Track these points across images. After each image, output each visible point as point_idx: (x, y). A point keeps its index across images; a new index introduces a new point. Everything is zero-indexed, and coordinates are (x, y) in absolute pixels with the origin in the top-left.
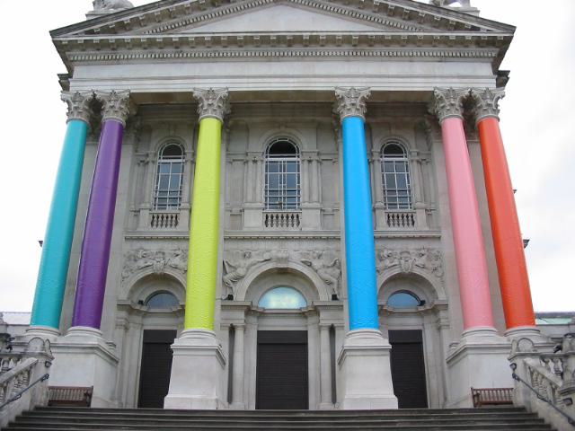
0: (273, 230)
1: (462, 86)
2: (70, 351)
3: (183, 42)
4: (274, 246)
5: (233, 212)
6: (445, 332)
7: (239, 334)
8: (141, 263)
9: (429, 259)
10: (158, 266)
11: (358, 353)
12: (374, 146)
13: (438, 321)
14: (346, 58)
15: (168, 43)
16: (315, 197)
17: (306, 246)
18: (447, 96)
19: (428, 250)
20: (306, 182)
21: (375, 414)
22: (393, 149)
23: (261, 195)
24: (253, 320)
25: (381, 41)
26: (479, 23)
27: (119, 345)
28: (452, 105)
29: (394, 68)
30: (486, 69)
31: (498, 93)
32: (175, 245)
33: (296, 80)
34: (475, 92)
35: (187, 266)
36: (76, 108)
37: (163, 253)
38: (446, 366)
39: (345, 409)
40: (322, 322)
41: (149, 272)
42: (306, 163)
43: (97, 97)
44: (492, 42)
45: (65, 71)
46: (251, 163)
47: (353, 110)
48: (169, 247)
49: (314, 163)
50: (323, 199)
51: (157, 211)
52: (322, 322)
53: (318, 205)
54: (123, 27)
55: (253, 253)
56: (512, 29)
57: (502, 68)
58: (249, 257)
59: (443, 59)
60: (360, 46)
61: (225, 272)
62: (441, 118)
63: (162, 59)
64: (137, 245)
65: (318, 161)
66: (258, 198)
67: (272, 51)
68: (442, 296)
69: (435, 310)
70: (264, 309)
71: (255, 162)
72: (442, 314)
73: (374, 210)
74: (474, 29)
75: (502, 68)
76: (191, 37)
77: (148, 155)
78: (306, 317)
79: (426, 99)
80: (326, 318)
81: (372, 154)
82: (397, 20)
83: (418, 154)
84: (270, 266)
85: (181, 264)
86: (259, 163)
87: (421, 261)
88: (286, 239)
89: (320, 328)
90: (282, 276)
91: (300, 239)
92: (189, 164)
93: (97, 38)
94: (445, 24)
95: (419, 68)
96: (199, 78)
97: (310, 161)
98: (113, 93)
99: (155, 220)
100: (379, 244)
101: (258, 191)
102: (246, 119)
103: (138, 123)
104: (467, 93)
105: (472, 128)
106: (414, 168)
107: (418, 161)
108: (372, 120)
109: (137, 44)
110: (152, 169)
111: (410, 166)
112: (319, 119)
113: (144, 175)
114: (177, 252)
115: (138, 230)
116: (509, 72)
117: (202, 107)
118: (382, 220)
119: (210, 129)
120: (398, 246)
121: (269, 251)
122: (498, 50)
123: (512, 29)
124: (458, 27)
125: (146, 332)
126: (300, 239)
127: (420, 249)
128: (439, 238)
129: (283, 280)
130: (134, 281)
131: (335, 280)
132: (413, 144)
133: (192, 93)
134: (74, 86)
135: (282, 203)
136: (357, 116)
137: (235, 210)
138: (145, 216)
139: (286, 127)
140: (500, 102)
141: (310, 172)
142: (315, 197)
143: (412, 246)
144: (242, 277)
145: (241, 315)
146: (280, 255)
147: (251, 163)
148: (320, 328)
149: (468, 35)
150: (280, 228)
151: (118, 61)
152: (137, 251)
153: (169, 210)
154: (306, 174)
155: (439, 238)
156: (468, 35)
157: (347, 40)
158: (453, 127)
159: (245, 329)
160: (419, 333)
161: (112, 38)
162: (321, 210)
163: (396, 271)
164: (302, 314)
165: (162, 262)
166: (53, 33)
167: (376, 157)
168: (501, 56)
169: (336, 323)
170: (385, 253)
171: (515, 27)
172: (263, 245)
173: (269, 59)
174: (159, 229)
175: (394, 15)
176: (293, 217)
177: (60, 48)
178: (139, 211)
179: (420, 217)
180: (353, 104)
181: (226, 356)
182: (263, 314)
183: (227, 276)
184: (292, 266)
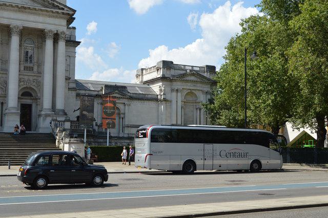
6: (38, 106)
29: (32, 18)
30: (64, 22)
44: (68, 14)
56: (75, 11)
59: (50, 16)
69: (36, 99)
72: (38, 100)
95: (40, 19)
120: (26, 78)
123: (75, 11)
149: (60, 11)
158: (49, 44)
170: (22, 80)
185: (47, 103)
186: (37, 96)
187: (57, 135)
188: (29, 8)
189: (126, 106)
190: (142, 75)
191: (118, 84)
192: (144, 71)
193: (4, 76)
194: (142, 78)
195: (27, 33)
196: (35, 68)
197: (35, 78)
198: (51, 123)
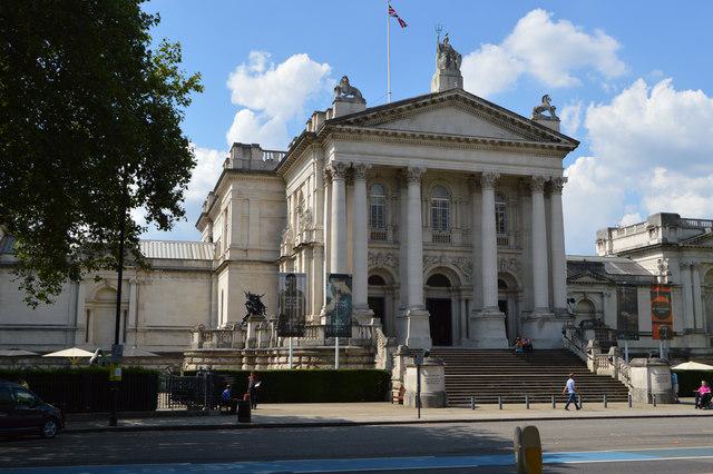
4: (439, 254)
6: (520, 304)
17: (454, 254)
29: (511, 158)
59: (538, 154)
74: (559, 141)
95: (523, 159)
185: (541, 300)
186: (517, 286)
187: (590, 352)
188: (510, 144)
189: (606, 299)
190: (611, 240)
191: (588, 259)
192: (614, 233)
193: (467, 255)
194: (611, 246)
195: (436, 179)
196: (390, 236)
197: (513, 256)
198: (564, 332)
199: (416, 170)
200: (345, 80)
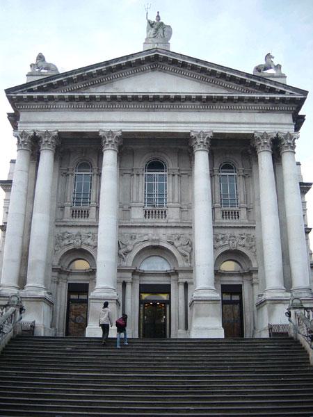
0: (150, 221)
1: (271, 130)
2: (28, 299)
3: (92, 98)
4: (151, 231)
5: (124, 208)
7: (129, 287)
8: (66, 242)
9: (247, 241)
10: (77, 243)
11: (201, 302)
12: (215, 165)
13: (252, 280)
14: (198, 110)
15: (82, 99)
16: (176, 199)
17: (170, 231)
18: (262, 137)
19: (247, 235)
20: (171, 189)
21: (211, 341)
22: (227, 167)
23: (141, 198)
24: (137, 277)
25: (220, 99)
26: (285, 88)
27: (54, 294)
28: (265, 143)
29: (228, 117)
30: (288, 119)
31: (295, 135)
32: (88, 230)
33: (165, 125)
34: (280, 135)
35: (97, 243)
36: (23, 142)
37: (81, 236)
38: (255, 308)
39: (193, 338)
40: (180, 280)
41: (71, 247)
42: (171, 176)
43: (37, 135)
44: (293, 101)
45: (12, 111)
46: (135, 176)
47: (202, 146)
48: (84, 231)
49: (176, 176)
50: (181, 200)
51: (75, 207)
52: (180, 280)
53: (179, 205)
54: (51, 87)
55: (137, 236)
56: (305, 93)
57: (300, 113)
58: (135, 239)
60: (208, 103)
61: (120, 248)
62: (258, 151)
63: (78, 109)
64: (64, 230)
65: (178, 175)
66: (140, 200)
67: (149, 105)
68: (254, 265)
70: (144, 271)
71: (138, 175)
72: (254, 276)
73: (213, 208)
75: (300, 113)
76: (97, 95)
77: (68, 170)
78: (170, 276)
79: (248, 138)
80: (182, 278)
81: (213, 171)
82: (233, 85)
83: (243, 171)
84: (148, 244)
85: (92, 243)
86: (141, 176)
87: (243, 242)
88: (158, 227)
89: (178, 284)
90: (156, 250)
91: (166, 227)
92: (95, 176)
93: (35, 95)
94: (262, 88)
95: (245, 117)
96: (103, 122)
97: (174, 175)
98: (47, 132)
99: (75, 213)
100: (217, 231)
101: (140, 195)
102: (131, 146)
103: (62, 149)
104: (275, 135)
105: (277, 158)
106: (241, 181)
107: (243, 176)
108: (214, 148)
109: (62, 99)
110: (71, 179)
111: (238, 178)
112: (179, 147)
113: (66, 183)
114: (89, 235)
115: (64, 220)
116: (305, 116)
117: (105, 142)
118: (219, 215)
119: (109, 157)
120: (228, 232)
121: (147, 235)
122: (296, 106)
123: (305, 93)
124: (272, 90)
125: (69, 284)
126: (166, 227)
127: (242, 235)
128: (255, 227)
129: (156, 252)
130: (62, 253)
131: (188, 254)
132: (240, 164)
133: (98, 133)
134: (21, 127)
135: (155, 209)
136: (204, 150)
137: (126, 207)
138: (68, 210)
139: (158, 151)
140: (296, 141)
141: (173, 181)
142: (176, 199)
143: (237, 232)
144: (131, 251)
145: (130, 275)
146: (154, 238)
147: (135, 176)
148: (178, 284)
149: (278, 96)
150: (157, 220)
151: (49, 109)
152: (63, 234)
153: (82, 207)
154: (171, 184)
155: (255, 227)
156: (278, 96)
157: (199, 99)
158: (265, 159)
159: (132, 283)
160: (240, 286)
161: (46, 95)
162: (180, 208)
163: (227, 248)
164: (168, 274)
165: (80, 241)
166: (8, 91)
167: (216, 173)
168: (299, 108)
169: (188, 281)
170: (220, 237)
171: (308, 92)
172: (143, 231)
173: (148, 110)
174: (77, 220)
175: (230, 81)
176: (162, 212)
177: (11, 100)
178: (64, 207)
179: (243, 213)
180: (202, 142)
181: (120, 301)
182: (142, 274)
183: (122, 253)
184: (162, 244)
193: (187, 231)
199: (111, 133)
200: (41, 57)
